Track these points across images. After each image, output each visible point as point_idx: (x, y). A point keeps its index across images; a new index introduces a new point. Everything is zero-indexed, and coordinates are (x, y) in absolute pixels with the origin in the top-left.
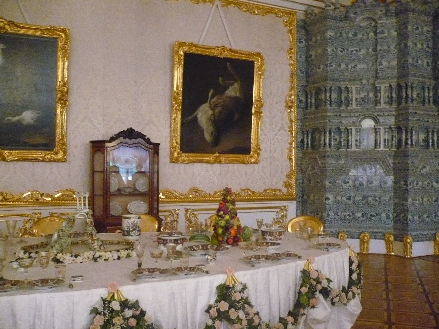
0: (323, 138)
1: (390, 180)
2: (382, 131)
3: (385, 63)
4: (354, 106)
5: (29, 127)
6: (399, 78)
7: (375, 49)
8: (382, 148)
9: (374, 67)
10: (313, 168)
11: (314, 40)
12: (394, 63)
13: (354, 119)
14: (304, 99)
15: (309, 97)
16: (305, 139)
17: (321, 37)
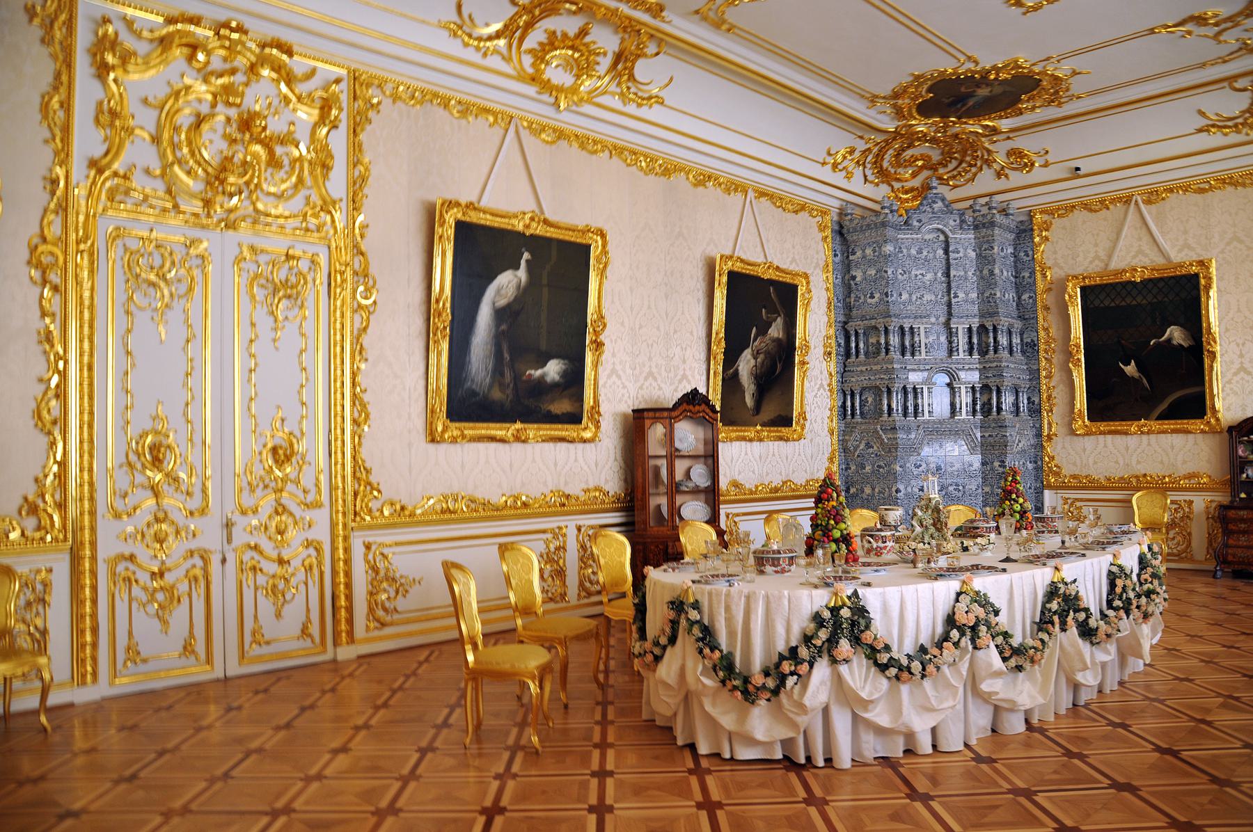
0: (885, 402)
1: (976, 460)
2: (963, 391)
3: (961, 295)
4: (923, 356)
5: (555, 386)
6: (982, 316)
7: (947, 274)
8: (964, 416)
9: (946, 298)
10: (868, 446)
11: (859, 254)
12: (974, 295)
13: (926, 374)
14: (842, 342)
15: (853, 338)
16: (849, 403)
17: (874, 251)
